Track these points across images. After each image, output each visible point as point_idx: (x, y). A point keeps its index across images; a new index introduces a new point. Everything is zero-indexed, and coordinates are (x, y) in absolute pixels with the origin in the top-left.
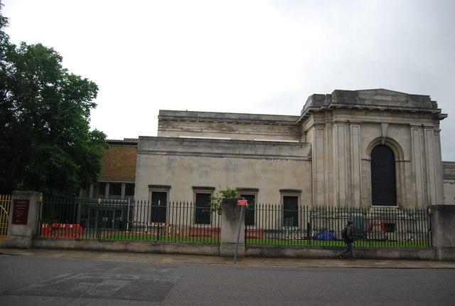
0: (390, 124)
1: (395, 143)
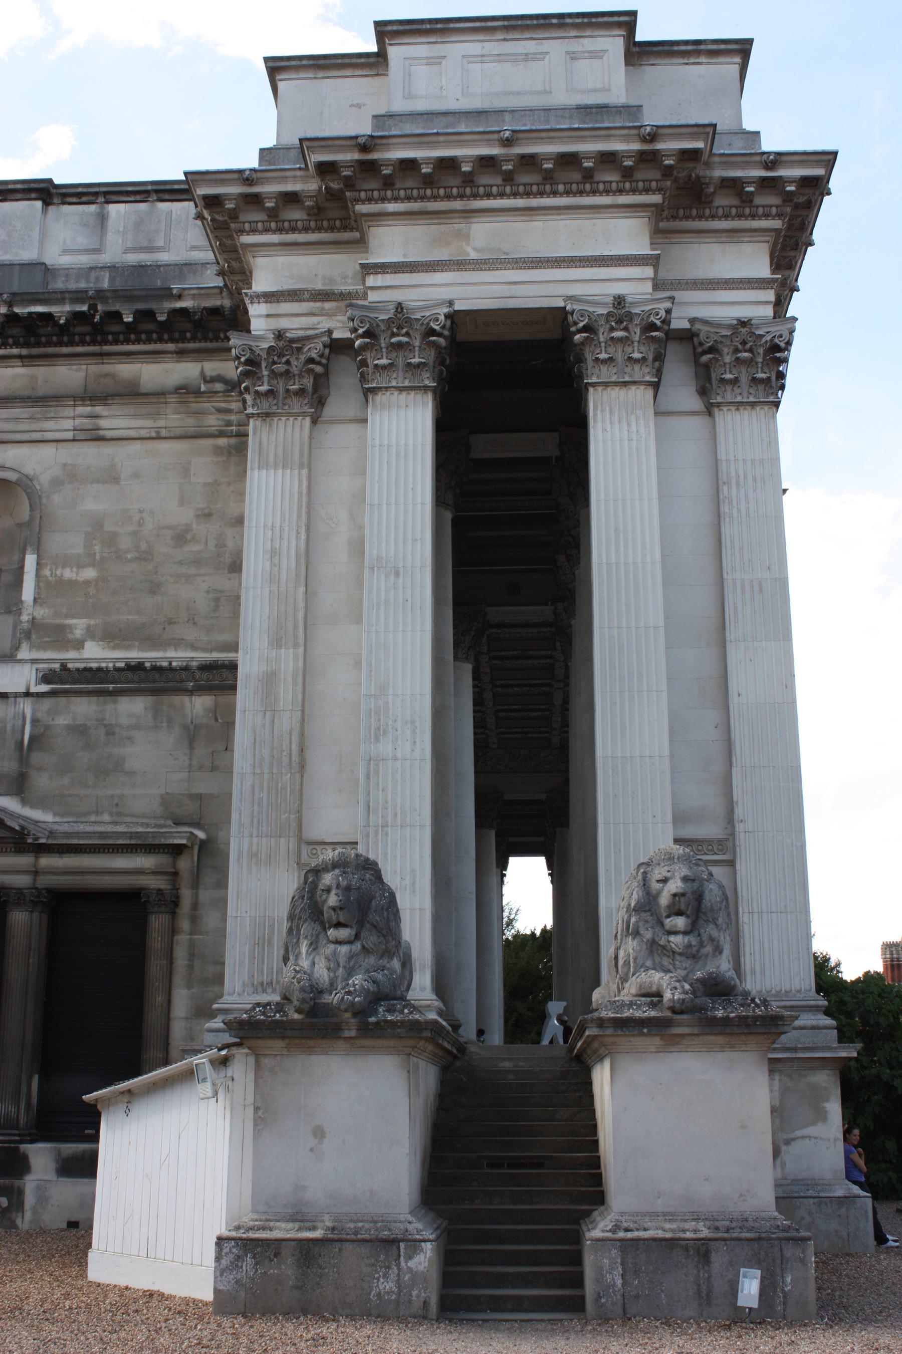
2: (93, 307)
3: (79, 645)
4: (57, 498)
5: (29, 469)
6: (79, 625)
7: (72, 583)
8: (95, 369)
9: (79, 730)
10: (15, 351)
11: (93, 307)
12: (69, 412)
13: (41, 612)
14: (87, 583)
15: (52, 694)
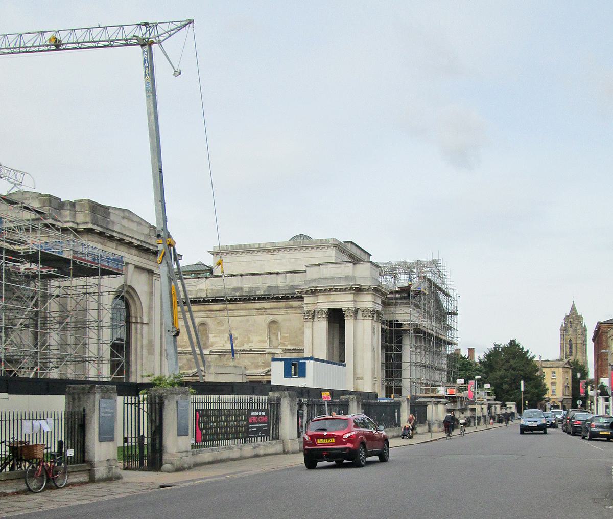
0: (137, 267)
1: (134, 295)
3: (287, 346)
5: (278, 319)
6: (287, 343)
8: (286, 303)
13: (282, 341)
14: (287, 337)
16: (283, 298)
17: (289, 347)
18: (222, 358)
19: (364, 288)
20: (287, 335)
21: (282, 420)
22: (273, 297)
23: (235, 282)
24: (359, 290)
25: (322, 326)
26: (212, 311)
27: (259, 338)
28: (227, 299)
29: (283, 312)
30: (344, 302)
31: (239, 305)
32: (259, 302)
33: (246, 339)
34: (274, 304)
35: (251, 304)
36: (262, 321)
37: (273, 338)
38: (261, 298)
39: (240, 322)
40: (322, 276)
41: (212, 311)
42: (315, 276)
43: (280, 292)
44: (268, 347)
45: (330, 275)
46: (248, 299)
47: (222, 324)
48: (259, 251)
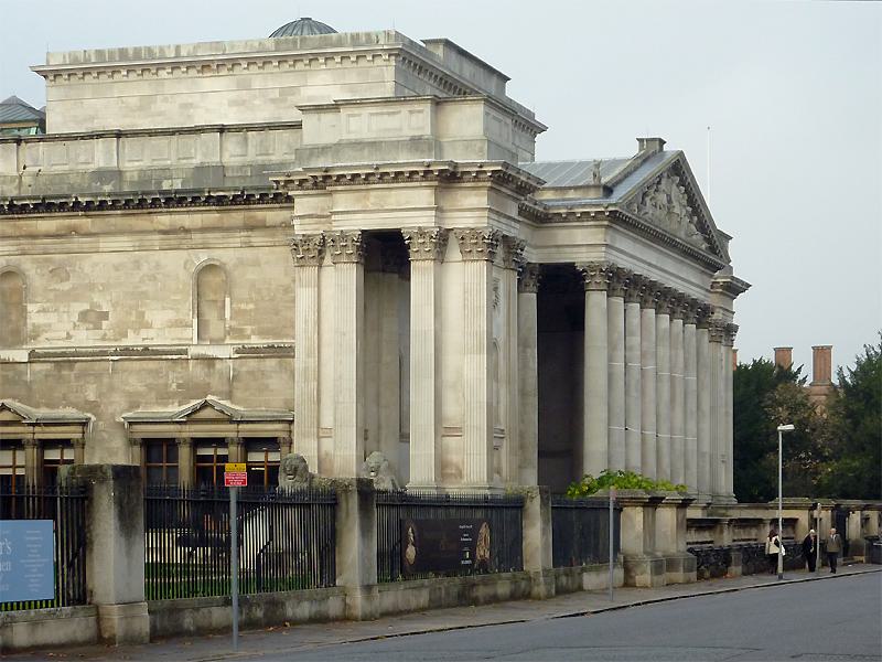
2: (243, 192)
3: (249, 337)
4: (236, 273)
5: (223, 260)
6: (248, 329)
7: (245, 311)
9: (251, 373)
10: (214, 207)
11: (243, 192)
12: (238, 234)
13: (234, 323)
14: (251, 310)
15: (240, 358)
16: (235, 200)
17: (256, 341)
18: (65, 372)
19: (463, 173)
20: (251, 306)
21: (95, 547)
22: (210, 197)
23: (100, 156)
24: (450, 178)
25: (342, 282)
26: (34, 236)
27: (170, 315)
28: (77, 203)
29: (238, 238)
30: (408, 210)
31: (112, 220)
32: (171, 213)
33: (133, 319)
34: (211, 217)
35: (147, 217)
36: (178, 264)
37: (211, 315)
38: (174, 200)
39: (117, 268)
40: (345, 137)
41: (34, 236)
42: (328, 138)
43: (229, 184)
44: (195, 342)
45: (367, 135)
46: (143, 201)
47: (64, 275)
48: (175, 66)
